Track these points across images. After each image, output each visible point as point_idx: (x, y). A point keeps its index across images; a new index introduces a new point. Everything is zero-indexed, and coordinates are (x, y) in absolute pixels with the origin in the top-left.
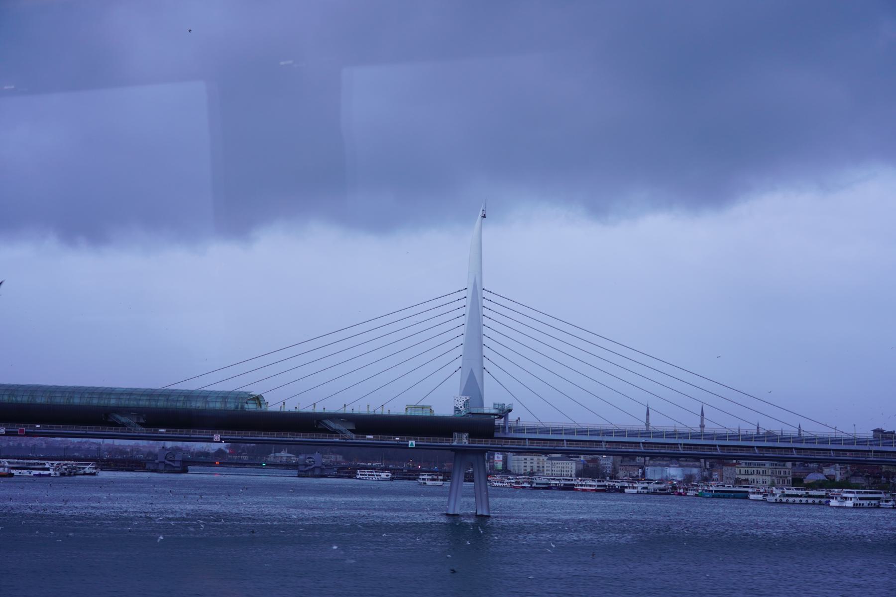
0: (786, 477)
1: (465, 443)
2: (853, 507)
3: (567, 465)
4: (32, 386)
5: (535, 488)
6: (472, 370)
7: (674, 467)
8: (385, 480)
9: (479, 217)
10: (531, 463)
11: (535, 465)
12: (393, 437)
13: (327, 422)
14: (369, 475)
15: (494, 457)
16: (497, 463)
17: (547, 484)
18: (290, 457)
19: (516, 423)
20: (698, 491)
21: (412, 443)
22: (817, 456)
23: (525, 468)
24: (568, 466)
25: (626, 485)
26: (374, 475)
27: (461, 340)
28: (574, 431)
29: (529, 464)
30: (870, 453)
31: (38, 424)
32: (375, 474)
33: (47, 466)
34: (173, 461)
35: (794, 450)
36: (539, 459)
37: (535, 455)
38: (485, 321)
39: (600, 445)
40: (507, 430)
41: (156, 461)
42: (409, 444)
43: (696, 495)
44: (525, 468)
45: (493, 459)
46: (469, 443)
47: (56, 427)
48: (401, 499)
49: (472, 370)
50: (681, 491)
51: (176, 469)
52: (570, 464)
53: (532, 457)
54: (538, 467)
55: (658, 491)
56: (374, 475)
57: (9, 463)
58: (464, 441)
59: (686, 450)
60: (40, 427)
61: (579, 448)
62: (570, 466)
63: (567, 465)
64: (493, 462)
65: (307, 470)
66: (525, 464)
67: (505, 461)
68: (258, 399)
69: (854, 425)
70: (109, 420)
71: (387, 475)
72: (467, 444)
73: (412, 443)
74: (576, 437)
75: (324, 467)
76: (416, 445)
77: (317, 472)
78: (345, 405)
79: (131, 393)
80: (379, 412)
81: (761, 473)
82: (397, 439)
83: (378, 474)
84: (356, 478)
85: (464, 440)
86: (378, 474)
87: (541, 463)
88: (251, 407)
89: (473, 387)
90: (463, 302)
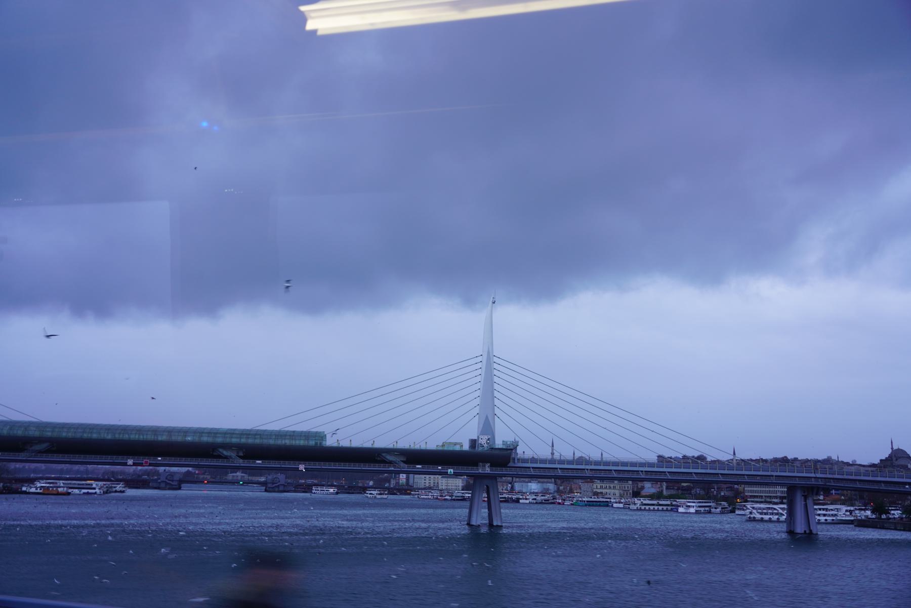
0: (629, 490)
1: (487, 471)
2: (695, 513)
3: (456, 482)
4: (90, 425)
5: (454, 500)
6: (487, 417)
7: (534, 483)
8: (332, 494)
9: (491, 303)
11: (432, 482)
13: (384, 454)
14: (321, 490)
17: (462, 497)
18: (244, 476)
20: (573, 501)
21: (451, 472)
25: (521, 497)
26: (324, 490)
27: (478, 393)
28: (609, 463)
29: (427, 481)
30: (772, 477)
31: (160, 457)
32: (325, 489)
33: (94, 486)
34: (173, 481)
36: (435, 478)
38: (496, 379)
39: (611, 473)
40: (516, 461)
41: (159, 481)
42: (449, 472)
43: (572, 504)
46: (490, 471)
47: (78, 457)
48: (382, 512)
49: (487, 417)
50: (560, 501)
51: (174, 487)
53: (430, 476)
55: (544, 501)
56: (324, 490)
57: (63, 483)
64: (399, 480)
65: (274, 487)
66: (425, 481)
67: (408, 479)
70: (215, 454)
71: (334, 491)
72: (489, 472)
73: (451, 472)
74: (548, 466)
75: (286, 484)
76: (454, 472)
77: (281, 488)
78: (338, 440)
79: (231, 433)
80: (423, 447)
81: (612, 488)
82: (440, 468)
83: (327, 489)
85: (487, 469)
86: (327, 489)
89: (487, 427)
90: (479, 365)
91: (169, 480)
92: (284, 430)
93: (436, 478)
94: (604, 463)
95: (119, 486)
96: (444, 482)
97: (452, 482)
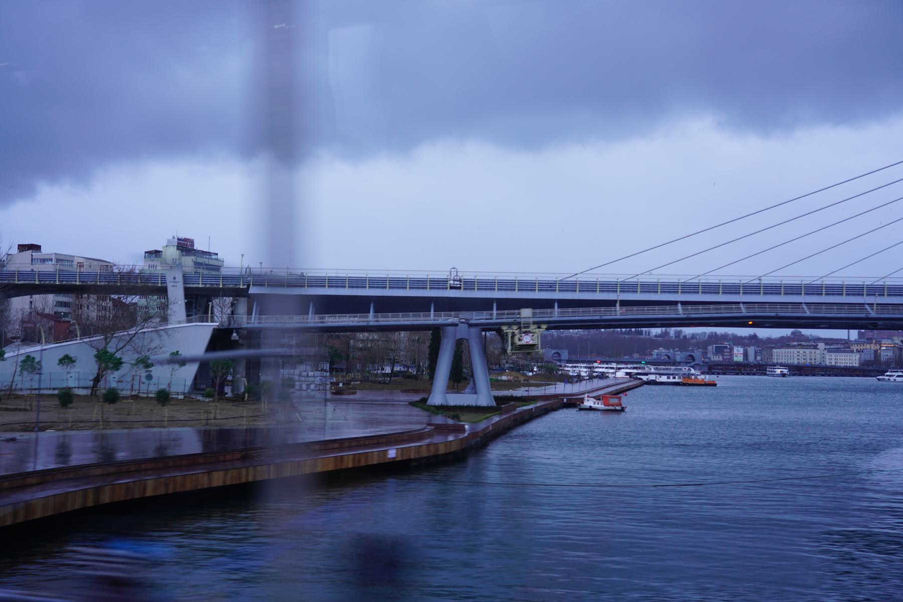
3: (851, 358)
10: (804, 356)
24: (852, 358)
36: (811, 352)
37: (806, 348)
52: (854, 356)
53: (805, 350)
54: (811, 359)
62: (854, 358)
63: (846, 358)
84: (765, 374)
87: (813, 355)
93: (813, 353)
96: (833, 356)
97: (846, 358)
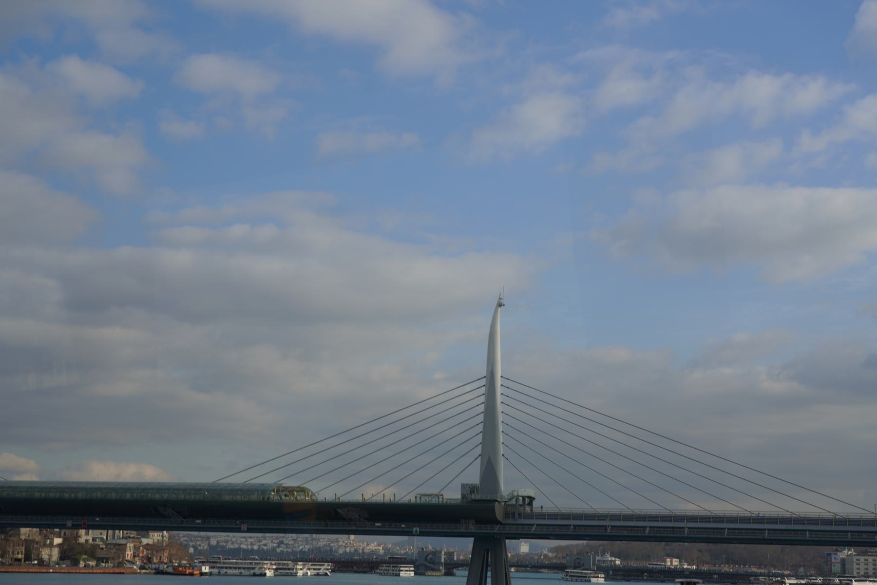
12: (399, 524)
15: (831, 558)
16: (834, 566)
19: (541, 509)
21: (416, 531)
22: (822, 537)
23: (858, 571)
35: (808, 532)
37: (869, 555)
40: (516, 516)
42: (414, 532)
44: (858, 571)
45: (831, 560)
49: (489, 459)
53: (866, 557)
58: (471, 527)
59: (665, 532)
60: (100, 519)
61: (633, 534)
68: (302, 490)
69: (875, 505)
72: (473, 531)
73: (416, 531)
76: (420, 532)
82: (403, 526)
88: (301, 498)
91: (430, 563)
92: (250, 484)
94: (636, 517)
95: (323, 568)
